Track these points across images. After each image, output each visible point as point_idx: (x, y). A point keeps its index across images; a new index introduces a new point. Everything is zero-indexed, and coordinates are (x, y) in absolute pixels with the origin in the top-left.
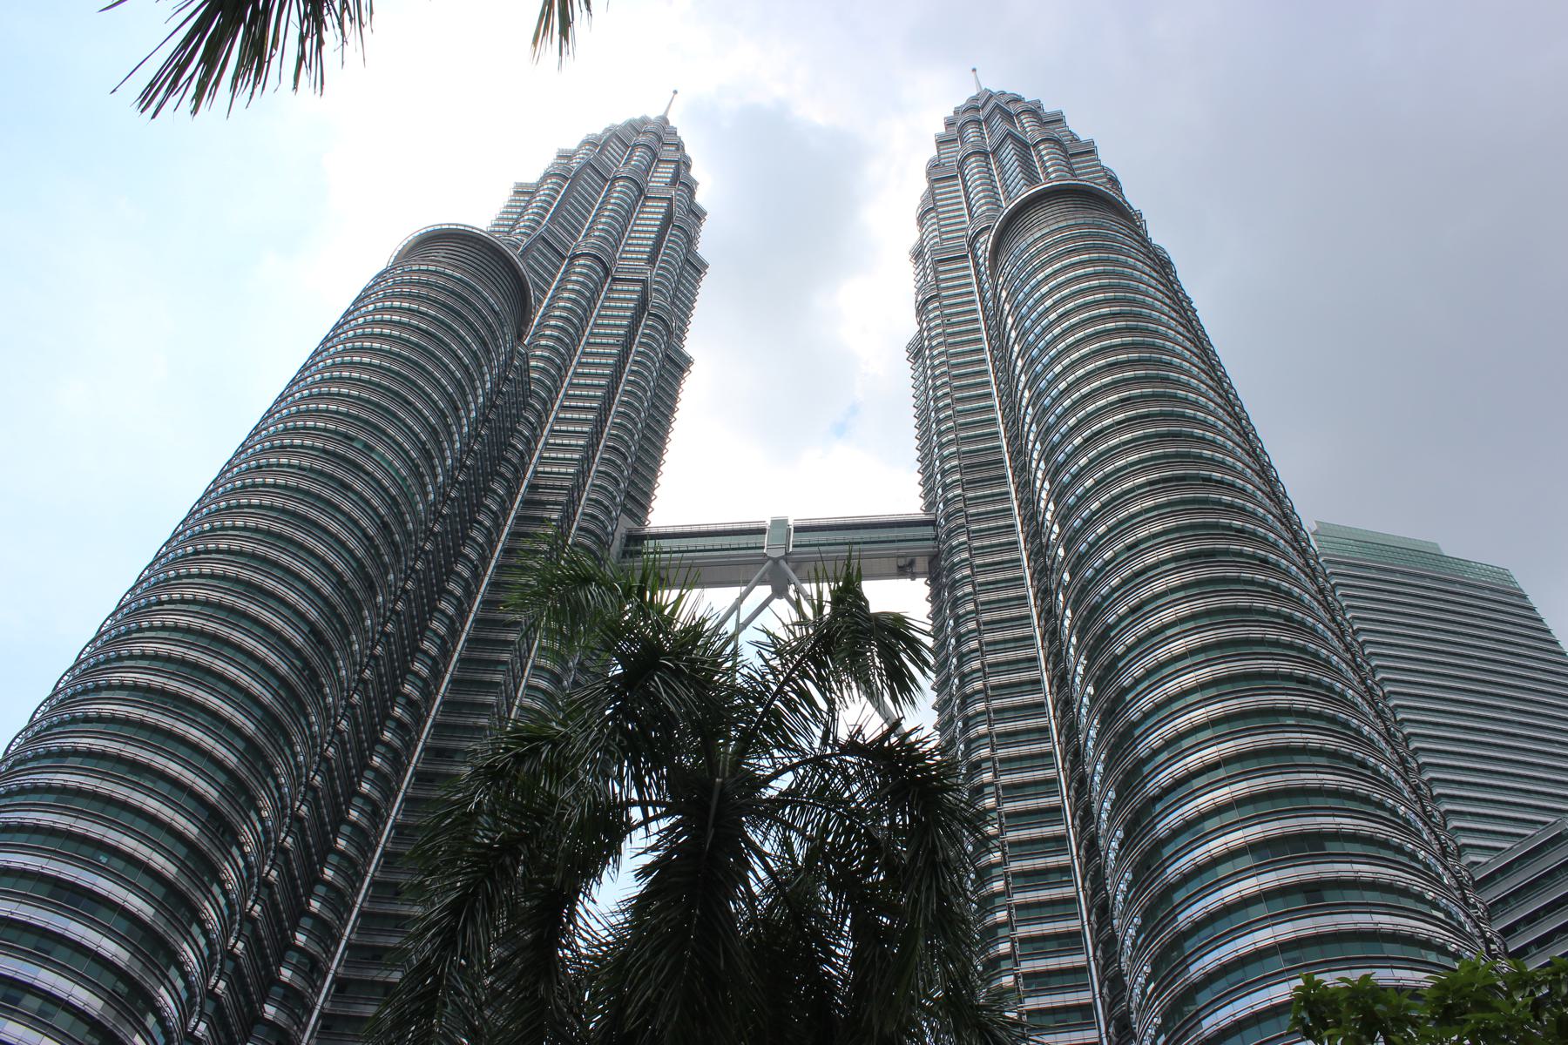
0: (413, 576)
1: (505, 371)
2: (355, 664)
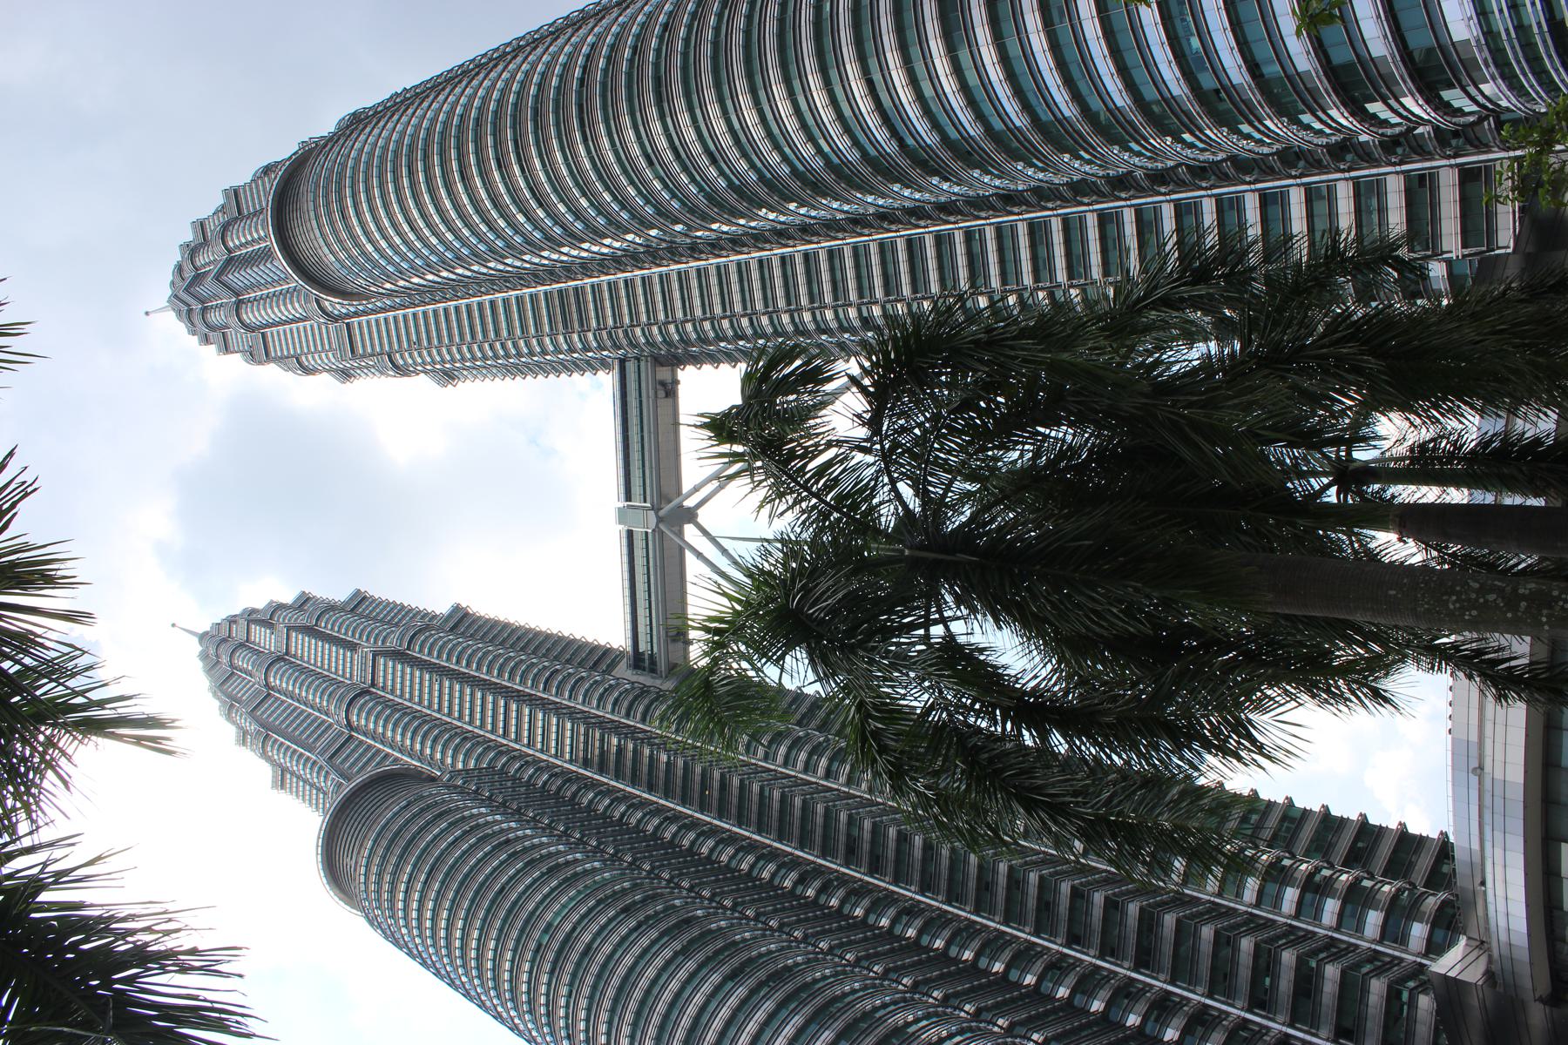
0: (676, 880)
1: (468, 794)
2: (764, 936)
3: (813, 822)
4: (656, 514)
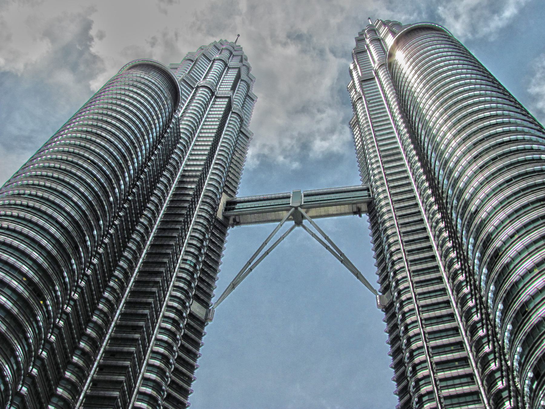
3: (120, 359)
4: (301, 206)
